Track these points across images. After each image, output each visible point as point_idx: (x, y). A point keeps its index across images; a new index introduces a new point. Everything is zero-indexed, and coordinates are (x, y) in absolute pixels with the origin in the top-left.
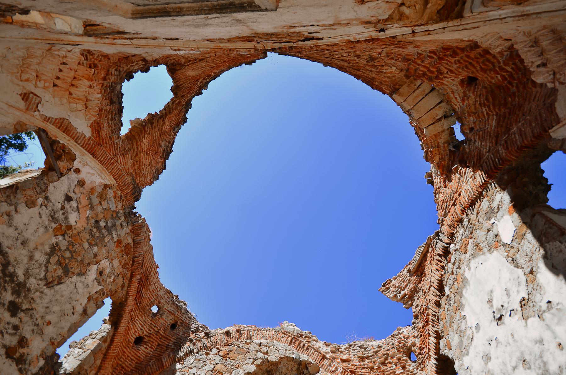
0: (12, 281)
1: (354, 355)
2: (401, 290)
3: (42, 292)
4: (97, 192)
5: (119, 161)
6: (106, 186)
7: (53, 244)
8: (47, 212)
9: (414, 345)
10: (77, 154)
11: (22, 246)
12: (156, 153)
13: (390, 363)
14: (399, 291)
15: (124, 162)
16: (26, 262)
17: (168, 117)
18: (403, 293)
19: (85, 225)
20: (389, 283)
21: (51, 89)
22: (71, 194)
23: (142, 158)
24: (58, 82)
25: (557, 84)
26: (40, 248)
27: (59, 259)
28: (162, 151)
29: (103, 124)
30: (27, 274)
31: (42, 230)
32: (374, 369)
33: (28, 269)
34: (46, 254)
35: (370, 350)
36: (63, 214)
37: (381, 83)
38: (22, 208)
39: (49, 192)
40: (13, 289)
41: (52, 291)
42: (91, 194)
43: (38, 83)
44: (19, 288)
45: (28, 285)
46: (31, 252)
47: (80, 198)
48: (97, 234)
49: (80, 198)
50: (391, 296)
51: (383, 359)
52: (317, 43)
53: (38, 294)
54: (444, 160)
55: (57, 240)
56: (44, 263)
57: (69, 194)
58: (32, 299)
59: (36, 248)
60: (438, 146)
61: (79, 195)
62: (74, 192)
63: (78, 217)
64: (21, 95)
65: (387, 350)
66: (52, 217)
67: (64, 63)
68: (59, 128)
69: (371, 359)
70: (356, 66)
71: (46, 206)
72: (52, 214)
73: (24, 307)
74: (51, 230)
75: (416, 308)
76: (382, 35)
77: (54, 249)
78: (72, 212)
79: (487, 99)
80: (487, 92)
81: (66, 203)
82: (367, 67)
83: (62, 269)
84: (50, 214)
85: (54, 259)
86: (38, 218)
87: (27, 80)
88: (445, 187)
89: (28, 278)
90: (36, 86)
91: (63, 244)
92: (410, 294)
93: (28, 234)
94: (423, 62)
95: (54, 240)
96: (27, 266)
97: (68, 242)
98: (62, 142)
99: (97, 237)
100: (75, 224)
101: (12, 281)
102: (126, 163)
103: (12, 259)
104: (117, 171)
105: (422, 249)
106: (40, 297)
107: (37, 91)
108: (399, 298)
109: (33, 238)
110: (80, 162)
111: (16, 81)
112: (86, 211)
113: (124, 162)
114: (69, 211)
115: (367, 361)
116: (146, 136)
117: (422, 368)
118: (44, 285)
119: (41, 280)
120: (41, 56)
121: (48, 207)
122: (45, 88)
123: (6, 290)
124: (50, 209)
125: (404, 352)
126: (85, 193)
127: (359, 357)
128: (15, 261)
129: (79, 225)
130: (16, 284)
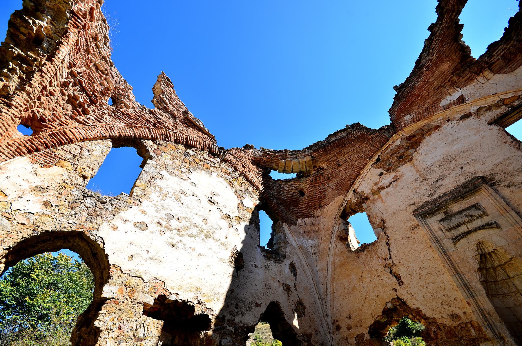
1: (96, 27)
2: (169, 99)
9: (127, 106)
13: (101, 77)
14: (168, 97)
18: (167, 101)
20: (171, 86)
25: (298, 226)
32: (88, 54)
35: (104, 50)
37: (321, 155)
50: (163, 88)
51: (103, 69)
52: (372, 161)
54: (263, 163)
60: (271, 162)
65: (111, 74)
69: (96, 51)
70: (339, 154)
75: (159, 113)
76: (352, 189)
79: (294, 198)
80: (297, 199)
82: (335, 158)
88: (249, 159)
92: (168, 109)
94: (323, 184)
105: (205, 129)
108: (162, 96)
115: (93, 45)
117: (111, 115)
125: (115, 94)
127: (97, 35)
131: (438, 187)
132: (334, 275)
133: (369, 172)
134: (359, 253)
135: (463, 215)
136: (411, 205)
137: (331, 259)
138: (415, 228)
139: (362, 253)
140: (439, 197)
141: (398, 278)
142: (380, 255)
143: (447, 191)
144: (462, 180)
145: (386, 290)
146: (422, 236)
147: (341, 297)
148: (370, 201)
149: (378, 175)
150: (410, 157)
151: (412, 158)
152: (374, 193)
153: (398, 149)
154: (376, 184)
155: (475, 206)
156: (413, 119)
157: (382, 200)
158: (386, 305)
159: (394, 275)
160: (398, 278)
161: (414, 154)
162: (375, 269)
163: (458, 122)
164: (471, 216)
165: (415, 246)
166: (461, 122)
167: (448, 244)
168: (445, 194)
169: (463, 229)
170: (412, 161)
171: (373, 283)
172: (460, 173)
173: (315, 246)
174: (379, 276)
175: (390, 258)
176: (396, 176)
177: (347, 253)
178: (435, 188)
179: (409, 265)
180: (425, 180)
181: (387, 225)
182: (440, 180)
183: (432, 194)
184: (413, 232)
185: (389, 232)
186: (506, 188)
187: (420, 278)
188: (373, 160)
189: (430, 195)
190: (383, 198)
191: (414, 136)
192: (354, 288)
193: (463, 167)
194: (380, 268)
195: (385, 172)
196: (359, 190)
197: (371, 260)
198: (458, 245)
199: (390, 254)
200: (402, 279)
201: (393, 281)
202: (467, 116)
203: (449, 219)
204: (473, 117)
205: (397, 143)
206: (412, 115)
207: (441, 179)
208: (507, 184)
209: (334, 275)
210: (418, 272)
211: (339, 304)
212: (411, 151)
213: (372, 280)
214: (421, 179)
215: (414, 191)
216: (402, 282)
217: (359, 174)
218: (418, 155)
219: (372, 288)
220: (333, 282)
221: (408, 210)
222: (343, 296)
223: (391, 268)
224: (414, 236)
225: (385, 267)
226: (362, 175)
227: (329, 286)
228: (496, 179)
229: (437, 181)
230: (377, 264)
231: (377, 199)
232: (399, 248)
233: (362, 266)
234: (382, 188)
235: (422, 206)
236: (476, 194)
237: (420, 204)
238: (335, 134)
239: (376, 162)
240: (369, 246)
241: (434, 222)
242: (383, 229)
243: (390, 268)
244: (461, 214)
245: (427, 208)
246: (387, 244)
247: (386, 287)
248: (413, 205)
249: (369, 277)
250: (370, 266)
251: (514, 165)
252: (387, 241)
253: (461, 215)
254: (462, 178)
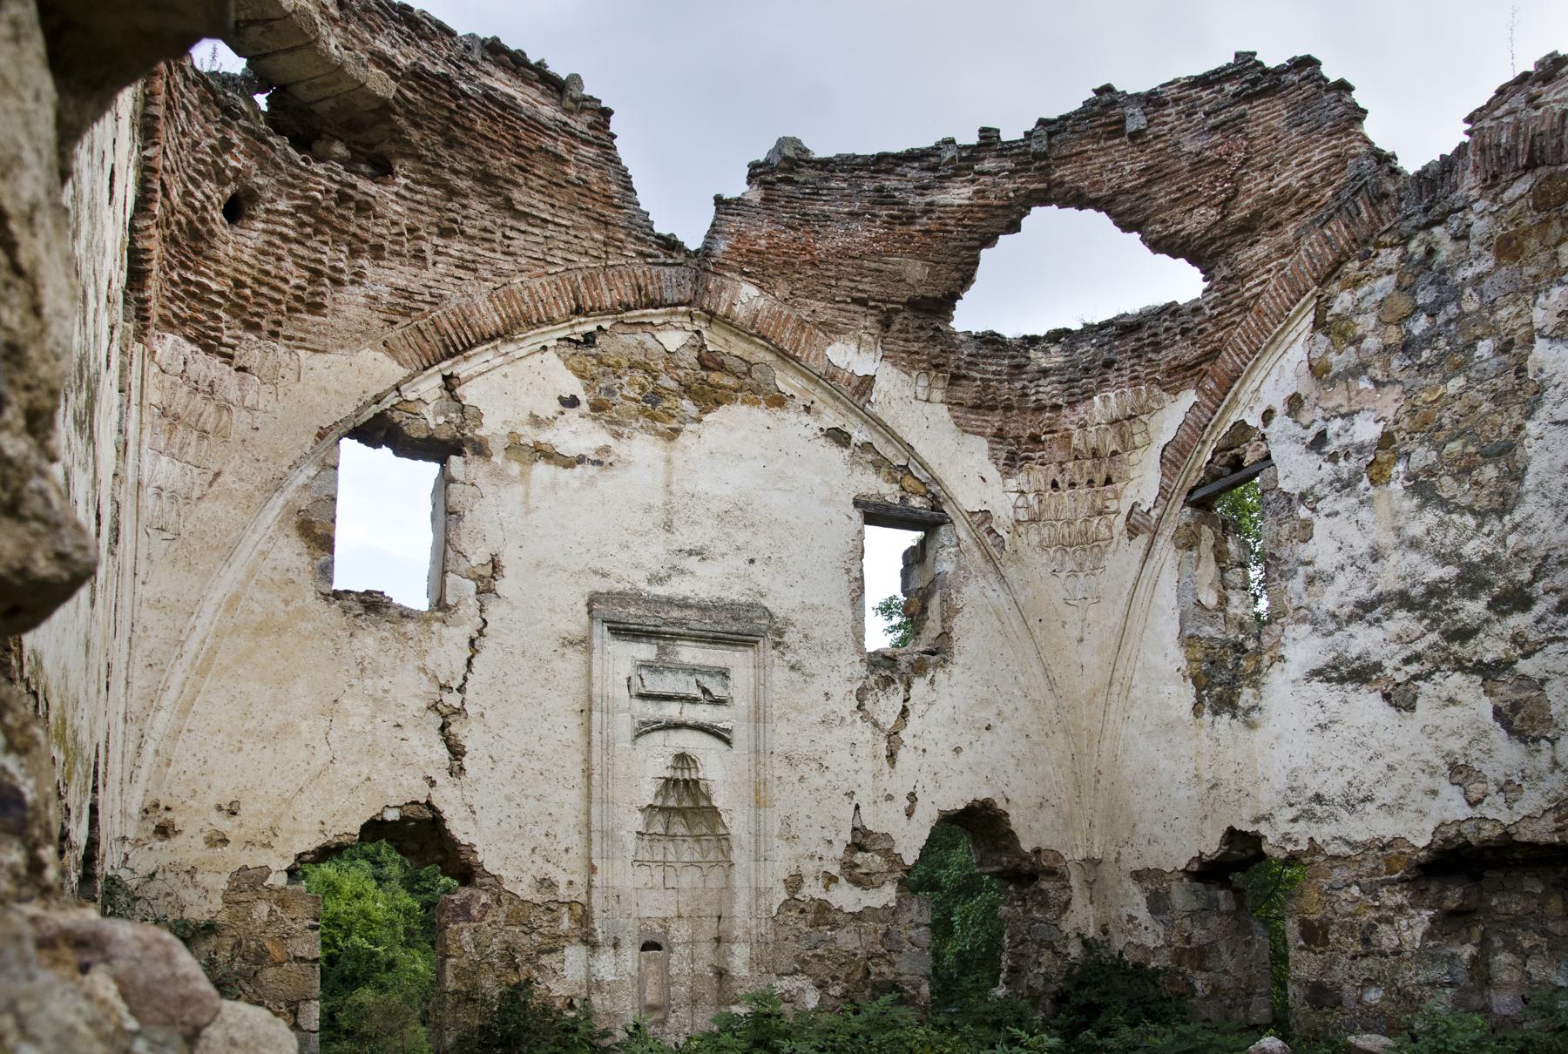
0: (1447, 592)
3: (1515, 527)
4: (1327, 351)
5: (1259, 289)
6: (1318, 324)
7: (1406, 488)
8: (1330, 498)
10: (1234, 417)
11: (1382, 560)
12: (1225, 162)
15: (1261, 271)
16: (1419, 557)
17: (1093, 195)
19: (1398, 388)
21: (1119, 486)
22: (1310, 435)
23: (1248, 207)
24: (1099, 478)
26: (1401, 521)
27: (1453, 475)
28: (1217, 137)
29: (1169, 362)
30: (1443, 559)
31: (1364, 515)
33: (1437, 555)
34: (1421, 508)
36: (1347, 456)
38: (1304, 551)
39: (1292, 492)
40: (1463, 595)
41: (1530, 498)
42: (1328, 372)
43: (1112, 509)
44: (1470, 580)
45: (1476, 559)
46: (1402, 543)
47: (1325, 410)
48: (1442, 343)
49: (1325, 410)
53: (1512, 540)
55: (1402, 476)
56: (1441, 514)
57: (1309, 439)
58: (1516, 555)
59: (1398, 530)
61: (1319, 413)
62: (1307, 427)
63: (1368, 414)
64: (1131, 539)
66: (1344, 487)
67: (1055, 485)
68: (1178, 468)
71: (1318, 500)
72: (1338, 485)
73: (1525, 575)
74: (1371, 492)
76: (446, 366)
77: (1422, 488)
78: (1350, 432)
81: (1327, 449)
83: (1485, 464)
84: (1338, 491)
85: (1447, 486)
86: (1336, 519)
87: (1109, 527)
89: (1460, 556)
90: (1117, 512)
91: (1423, 456)
93: (1361, 545)
95: (1397, 487)
96: (1428, 556)
97: (1421, 443)
98: (1209, 457)
99: (1448, 344)
100: (1382, 423)
101: (1447, 592)
102: (1264, 264)
103: (1398, 586)
104: (1279, 296)
106: (1526, 534)
107: (1125, 512)
109: (1373, 536)
110: (1251, 409)
111: (1113, 546)
112: (1359, 392)
113: (1261, 271)
114: (1345, 440)
116: (1172, 230)
118: (1501, 519)
119: (1480, 526)
120: (1053, 526)
121: (1322, 494)
122: (1117, 497)
123: (1456, 611)
124: (1327, 490)
126: (1317, 395)
128: (1404, 579)
129: (1390, 414)
130: (1458, 585)
131: (682, 572)
132: (213, 651)
133: (538, 356)
134: (358, 622)
135: (692, 680)
136: (596, 572)
137: (229, 578)
138: (571, 643)
139: (373, 629)
140: (670, 602)
141: (456, 751)
142: (431, 666)
143: (692, 595)
144: (736, 593)
145: (402, 772)
146: (575, 674)
147: (220, 737)
148: (486, 468)
149: (561, 399)
150: (674, 424)
151: (677, 431)
152: (515, 447)
153: (661, 366)
154: (536, 421)
155: (724, 674)
156: (756, 316)
157: (527, 495)
158: (382, 814)
159: (447, 741)
160: (456, 751)
161: (690, 427)
162: (395, 699)
163: (819, 434)
164: (705, 691)
165: (545, 691)
166: (822, 441)
167: (624, 727)
168: (684, 604)
169: (672, 711)
170: (672, 444)
171: (370, 739)
172: (742, 573)
173: (173, 496)
174: (398, 725)
175: (461, 689)
176: (606, 450)
177: (310, 596)
178: (674, 568)
179: (504, 733)
180: (668, 527)
181: (501, 586)
182: (698, 554)
183: (661, 579)
184: (560, 651)
185: (494, 611)
186: (787, 670)
187: (514, 777)
188: (577, 329)
189: (655, 579)
190: (536, 491)
191: (721, 367)
192: (286, 729)
193: (757, 563)
194: (416, 706)
195: (585, 407)
196: (470, 394)
197: (394, 669)
198: (640, 740)
199: (465, 679)
200: (466, 761)
201: (435, 757)
202: (839, 437)
203: (662, 673)
204: (847, 452)
205: (673, 340)
206: (762, 302)
207: (699, 553)
208: (793, 661)
209: (213, 651)
210: (517, 759)
211: (200, 756)
212: (687, 405)
213: (369, 728)
214: (659, 516)
215: (627, 537)
216: (462, 769)
217: (504, 334)
218: (694, 438)
219: (360, 751)
220: (202, 673)
221: (582, 581)
222: (230, 736)
223: (446, 721)
224: (557, 663)
225: (433, 707)
226: (511, 347)
227: (176, 680)
228: (785, 639)
229: (690, 553)
230: (410, 690)
231: (513, 481)
232: (501, 674)
233: (355, 671)
234: (546, 454)
235: (619, 593)
236: (741, 648)
237: (619, 587)
238: (515, 63)
239: (577, 342)
240: (402, 616)
241: (624, 657)
242: (478, 593)
243: (445, 717)
244: (691, 674)
245: (632, 610)
246: (472, 642)
247: (405, 764)
248: (604, 575)
249: (362, 715)
250: (384, 683)
251: (826, 630)
252: (476, 635)
253: (689, 678)
254: (736, 588)
